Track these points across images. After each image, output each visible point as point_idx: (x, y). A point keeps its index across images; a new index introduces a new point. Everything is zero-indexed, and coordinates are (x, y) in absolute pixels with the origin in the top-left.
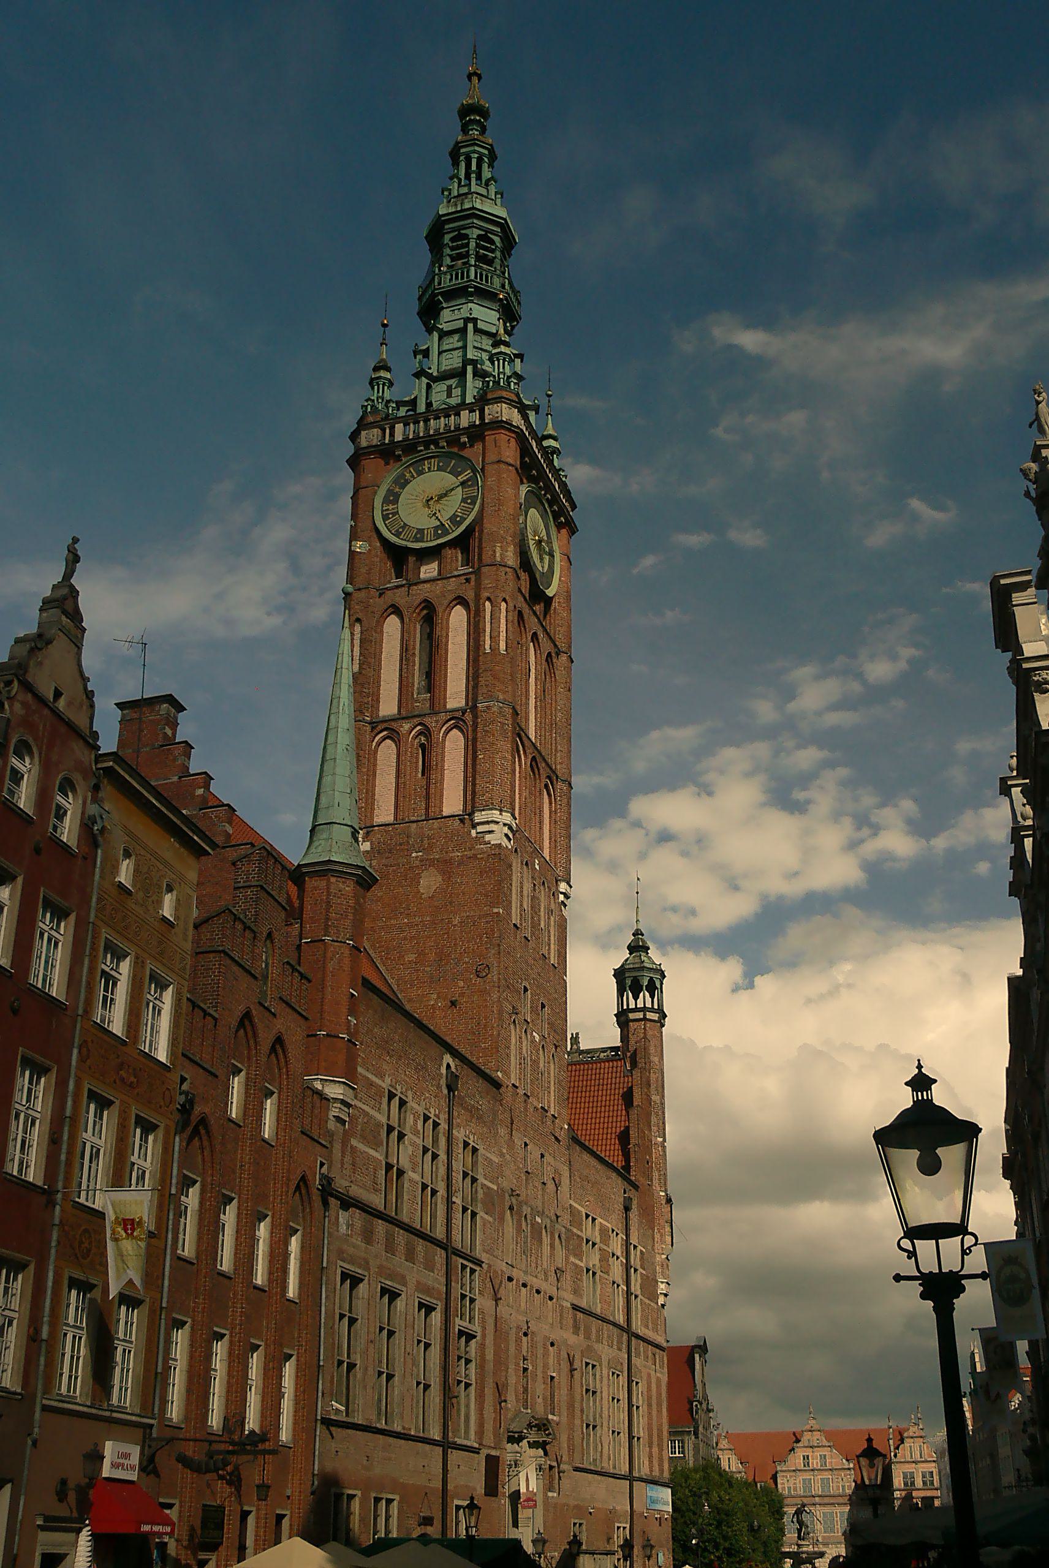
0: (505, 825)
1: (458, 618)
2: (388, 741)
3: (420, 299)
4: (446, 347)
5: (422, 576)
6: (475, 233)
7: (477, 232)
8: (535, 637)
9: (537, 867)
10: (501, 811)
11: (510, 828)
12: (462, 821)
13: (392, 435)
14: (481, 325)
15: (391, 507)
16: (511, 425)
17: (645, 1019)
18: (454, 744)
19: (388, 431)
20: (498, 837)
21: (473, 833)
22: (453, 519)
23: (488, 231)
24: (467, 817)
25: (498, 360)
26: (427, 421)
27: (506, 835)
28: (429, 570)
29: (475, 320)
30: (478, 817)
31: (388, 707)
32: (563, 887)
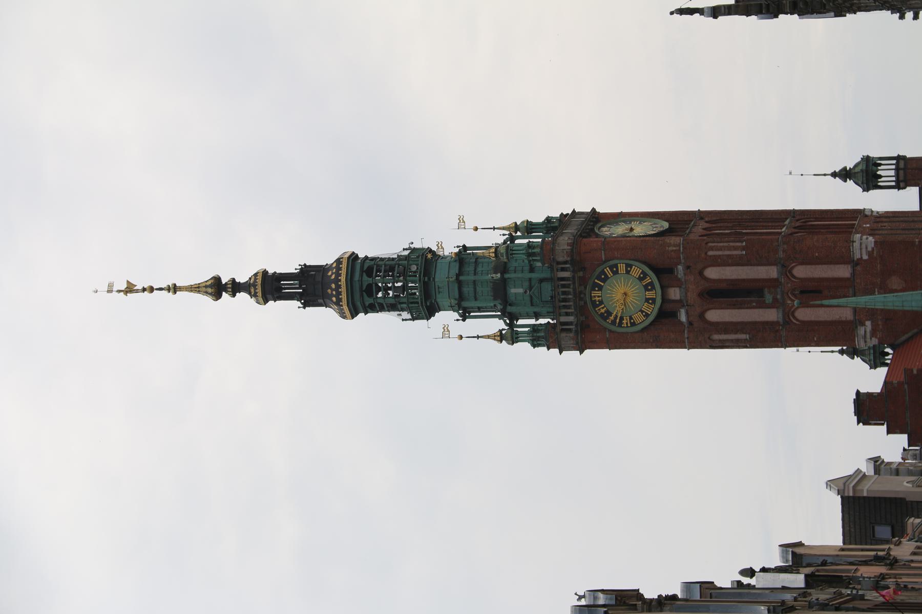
1: (712, 273)
2: (797, 314)
3: (413, 319)
4: (472, 294)
5: (678, 297)
6: (367, 280)
7: (365, 277)
12: (857, 264)
14: (455, 269)
15: (625, 322)
17: (904, 169)
18: (801, 271)
21: (865, 257)
22: (640, 279)
23: (362, 271)
28: (675, 294)
31: (772, 315)
32: (867, 213)
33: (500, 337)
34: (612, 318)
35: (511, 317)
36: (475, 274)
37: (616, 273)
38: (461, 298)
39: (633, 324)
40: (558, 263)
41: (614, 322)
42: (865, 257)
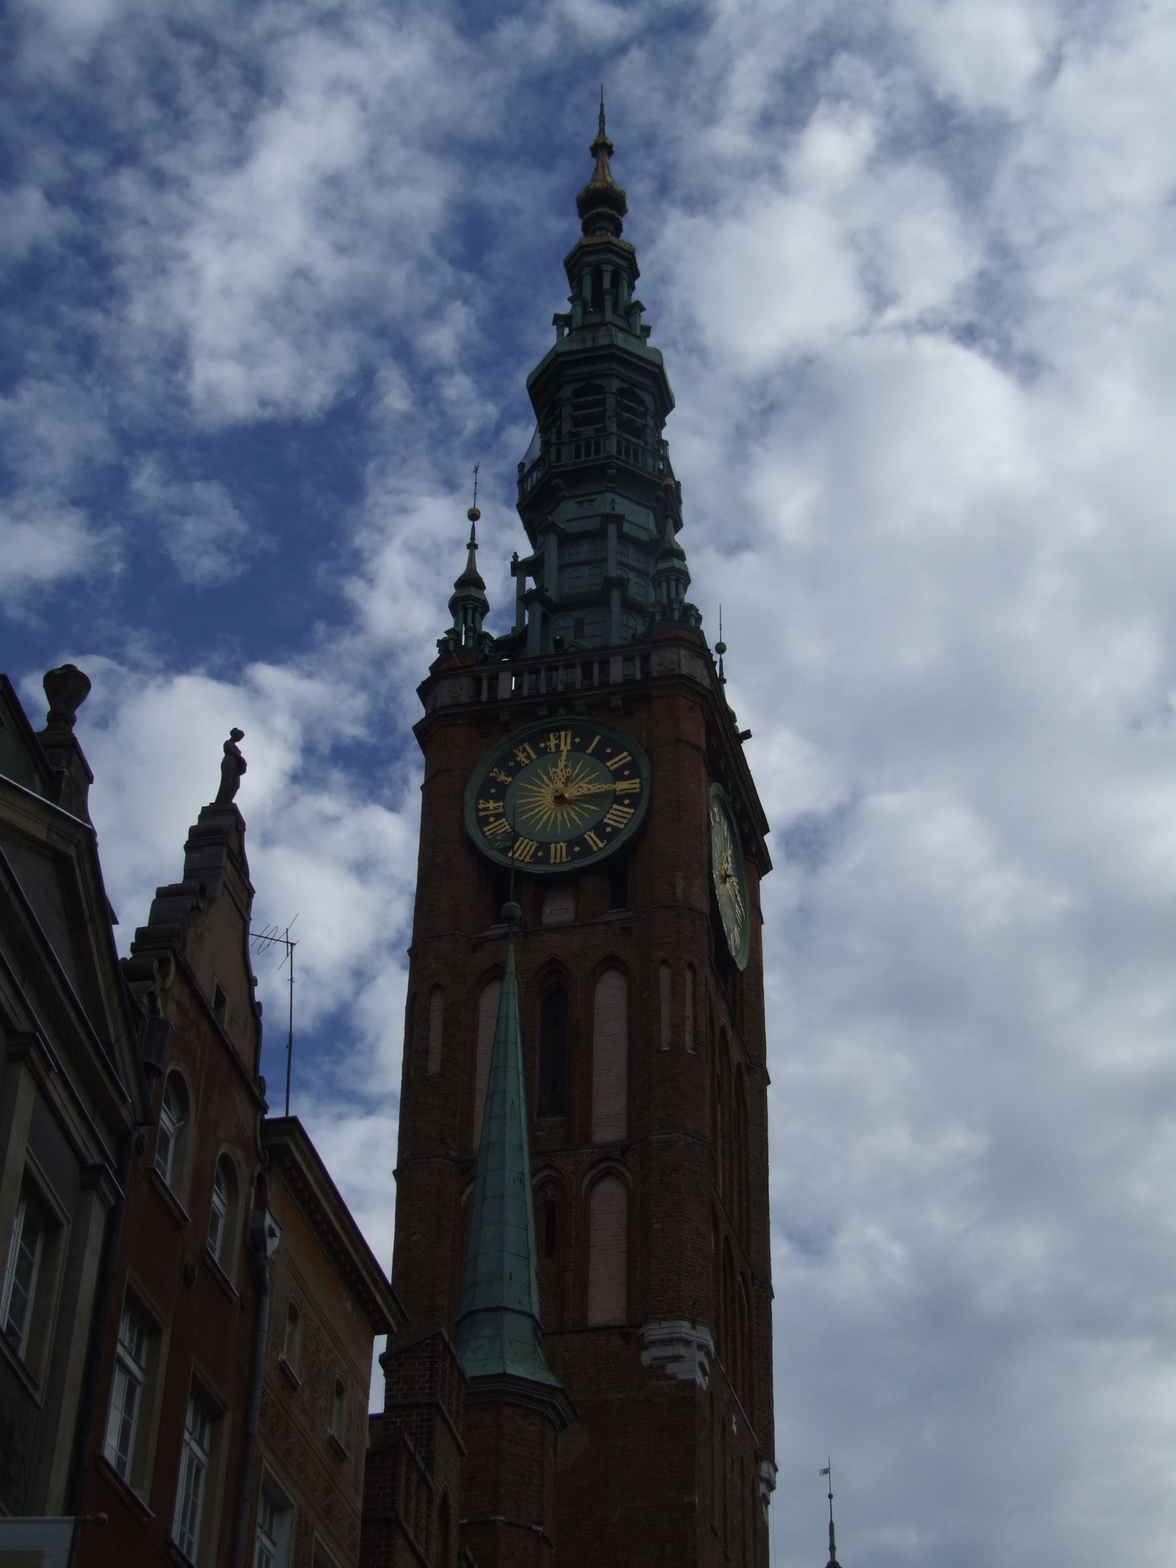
0: (700, 1347)
3: (521, 482)
7: (616, 385)
8: (723, 1029)
9: (734, 1428)
10: (694, 1323)
11: (708, 1353)
13: (493, 689)
14: (627, 528)
15: (491, 805)
16: (696, 683)
18: (608, 1207)
19: (485, 684)
20: (693, 1368)
21: (646, 1358)
24: (629, 1332)
25: (668, 581)
26: (552, 668)
27: (701, 1365)
28: (558, 910)
29: (619, 519)
30: (654, 1331)
32: (765, 1467)
33: (470, 582)
34: (502, 777)
35: (514, 643)
36: (620, 563)
37: (617, 776)
38: (567, 540)
39: (483, 822)
40: (645, 659)
41: (492, 781)
42: (646, 1358)
